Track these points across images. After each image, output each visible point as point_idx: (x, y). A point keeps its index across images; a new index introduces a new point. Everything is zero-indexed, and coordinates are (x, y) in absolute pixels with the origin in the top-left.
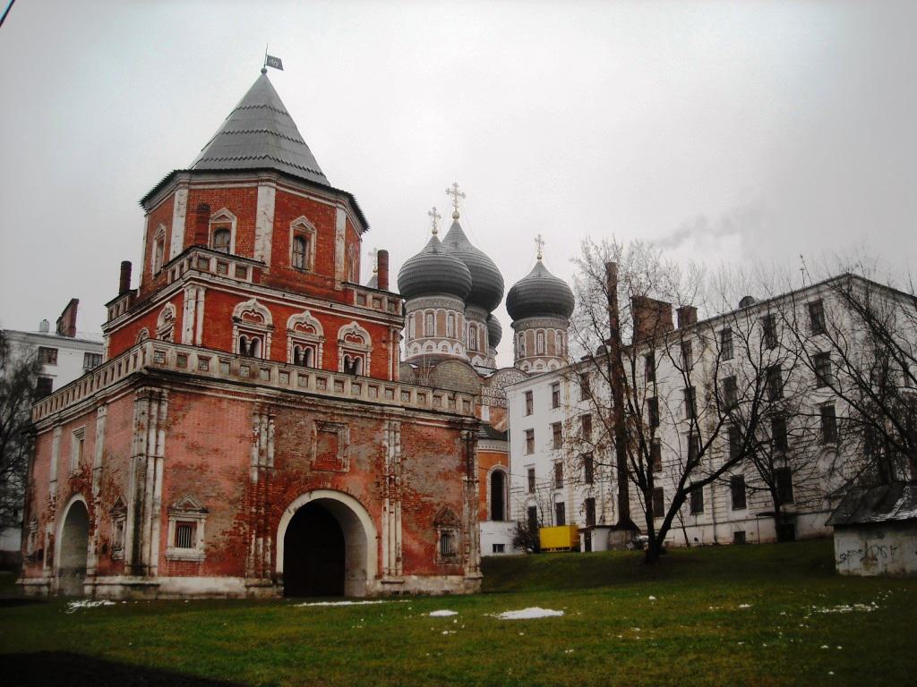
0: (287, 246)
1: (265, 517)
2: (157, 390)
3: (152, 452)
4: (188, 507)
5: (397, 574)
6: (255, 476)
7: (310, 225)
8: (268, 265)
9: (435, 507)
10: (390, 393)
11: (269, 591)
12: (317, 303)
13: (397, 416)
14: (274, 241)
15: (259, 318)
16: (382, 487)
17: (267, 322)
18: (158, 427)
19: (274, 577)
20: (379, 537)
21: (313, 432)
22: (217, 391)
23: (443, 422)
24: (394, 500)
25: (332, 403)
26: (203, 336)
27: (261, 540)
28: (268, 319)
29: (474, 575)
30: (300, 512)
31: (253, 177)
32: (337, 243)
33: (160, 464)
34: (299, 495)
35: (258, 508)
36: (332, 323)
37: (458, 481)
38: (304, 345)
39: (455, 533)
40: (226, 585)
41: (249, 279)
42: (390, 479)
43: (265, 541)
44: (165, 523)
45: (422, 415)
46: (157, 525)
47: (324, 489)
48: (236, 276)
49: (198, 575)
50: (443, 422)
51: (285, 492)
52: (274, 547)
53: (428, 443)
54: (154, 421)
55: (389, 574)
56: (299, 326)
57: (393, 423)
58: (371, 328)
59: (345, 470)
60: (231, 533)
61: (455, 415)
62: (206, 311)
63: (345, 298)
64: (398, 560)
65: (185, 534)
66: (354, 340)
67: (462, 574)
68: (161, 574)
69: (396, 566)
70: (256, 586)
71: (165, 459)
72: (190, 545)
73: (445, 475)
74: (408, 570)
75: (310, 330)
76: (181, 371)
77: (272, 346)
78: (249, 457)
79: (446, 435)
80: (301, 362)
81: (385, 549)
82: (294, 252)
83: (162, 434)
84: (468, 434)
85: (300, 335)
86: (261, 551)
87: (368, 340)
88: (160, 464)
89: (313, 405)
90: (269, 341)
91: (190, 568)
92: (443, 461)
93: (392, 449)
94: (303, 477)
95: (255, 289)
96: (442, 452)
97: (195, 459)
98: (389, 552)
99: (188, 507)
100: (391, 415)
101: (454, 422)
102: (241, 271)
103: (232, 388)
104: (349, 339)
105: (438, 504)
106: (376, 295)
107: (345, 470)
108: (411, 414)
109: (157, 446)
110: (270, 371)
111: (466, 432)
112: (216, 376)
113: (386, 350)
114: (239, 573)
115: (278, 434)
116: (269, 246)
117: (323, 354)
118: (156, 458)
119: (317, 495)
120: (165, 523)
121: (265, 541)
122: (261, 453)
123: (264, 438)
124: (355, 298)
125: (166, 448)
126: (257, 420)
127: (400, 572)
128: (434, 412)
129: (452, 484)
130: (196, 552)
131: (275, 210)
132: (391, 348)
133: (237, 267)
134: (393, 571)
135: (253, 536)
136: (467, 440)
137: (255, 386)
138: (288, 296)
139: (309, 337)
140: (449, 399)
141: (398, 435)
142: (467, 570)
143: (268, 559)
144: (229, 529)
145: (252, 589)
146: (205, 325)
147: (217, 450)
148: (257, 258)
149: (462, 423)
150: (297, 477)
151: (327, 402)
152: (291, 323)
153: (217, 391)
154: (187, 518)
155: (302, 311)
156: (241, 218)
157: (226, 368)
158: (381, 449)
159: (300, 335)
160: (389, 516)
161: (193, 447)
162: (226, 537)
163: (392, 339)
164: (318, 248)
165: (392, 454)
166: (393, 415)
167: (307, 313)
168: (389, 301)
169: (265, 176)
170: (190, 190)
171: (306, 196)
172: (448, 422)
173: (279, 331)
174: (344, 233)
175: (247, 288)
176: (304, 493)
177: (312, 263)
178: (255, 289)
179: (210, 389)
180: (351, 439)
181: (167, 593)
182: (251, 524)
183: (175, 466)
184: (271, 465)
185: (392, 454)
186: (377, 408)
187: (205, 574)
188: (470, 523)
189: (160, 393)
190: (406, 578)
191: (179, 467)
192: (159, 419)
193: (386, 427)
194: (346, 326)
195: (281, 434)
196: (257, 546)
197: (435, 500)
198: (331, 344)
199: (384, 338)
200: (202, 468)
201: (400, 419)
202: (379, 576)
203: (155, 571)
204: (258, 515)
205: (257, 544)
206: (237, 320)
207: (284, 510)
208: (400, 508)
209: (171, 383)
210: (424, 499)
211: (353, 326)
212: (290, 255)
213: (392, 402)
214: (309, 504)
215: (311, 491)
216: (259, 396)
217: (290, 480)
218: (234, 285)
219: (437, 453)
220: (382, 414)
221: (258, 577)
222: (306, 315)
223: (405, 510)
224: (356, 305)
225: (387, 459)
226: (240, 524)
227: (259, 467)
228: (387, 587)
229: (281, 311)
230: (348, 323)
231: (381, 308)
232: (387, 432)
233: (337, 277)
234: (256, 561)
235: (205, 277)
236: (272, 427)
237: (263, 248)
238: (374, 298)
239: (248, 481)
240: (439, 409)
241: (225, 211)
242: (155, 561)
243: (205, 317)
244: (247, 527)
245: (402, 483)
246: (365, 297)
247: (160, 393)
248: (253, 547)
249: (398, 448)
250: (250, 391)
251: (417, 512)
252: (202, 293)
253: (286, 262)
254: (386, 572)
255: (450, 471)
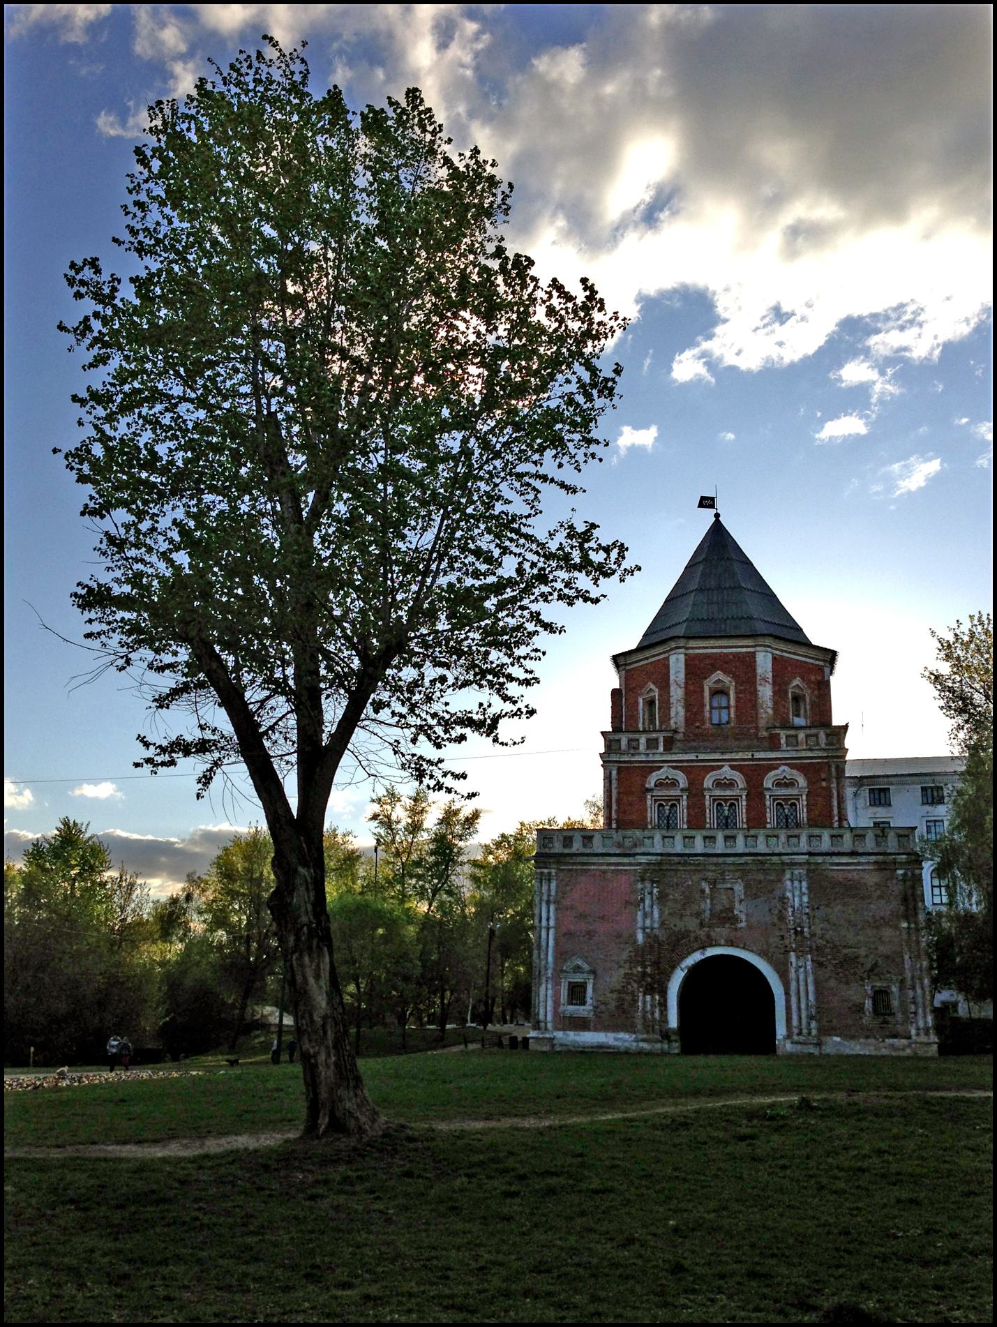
0: (703, 705)
1: (650, 976)
2: (546, 871)
3: (544, 923)
4: (577, 969)
5: (809, 1034)
6: (640, 937)
7: (727, 679)
8: (682, 730)
9: (861, 960)
10: (794, 840)
11: (658, 1046)
12: (734, 756)
13: (800, 864)
14: (688, 706)
15: (674, 783)
16: (787, 942)
17: (682, 786)
18: (548, 902)
19: (666, 1036)
20: (787, 994)
21: (703, 891)
22: (602, 864)
23: (868, 863)
24: (801, 954)
25: (721, 860)
26: (617, 812)
27: (648, 998)
28: (682, 780)
29: (923, 1039)
30: (694, 971)
31: (659, 650)
32: (759, 688)
33: (552, 932)
34: (689, 954)
35: (644, 967)
36: (754, 774)
37: (897, 927)
38: (726, 801)
39: (894, 989)
40: (616, 1039)
41: (661, 749)
42: (796, 932)
43: (653, 998)
44: (557, 984)
45: (836, 860)
46: (550, 986)
47: (720, 945)
48: (648, 748)
49: (589, 1030)
50: (868, 863)
51: (673, 951)
52: (663, 1005)
53: (851, 889)
54: (545, 898)
55: (800, 1034)
56: (719, 784)
57: (796, 872)
58: (802, 768)
59: (740, 925)
60: (619, 992)
61: (885, 854)
62: (618, 787)
63: (774, 744)
64: (811, 1018)
65: (577, 992)
66: (786, 785)
67: (909, 1038)
68: (556, 1029)
69: (809, 1024)
70: (644, 1040)
71: (557, 928)
72: (584, 1003)
73: (878, 924)
74: (825, 1031)
75: (731, 784)
76: (566, 851)
77: (688, 807)
78: (635, 920)
79: (872, 879)
80: (726, 823)
81: (794, 1007)
82: (711, 708)
83: (552, 908)
84: (905, 874)
85: (718, 792)
86: (649, 1007)
87: (802, 781)
88: (552, 932)
89: (699, 865)
90: (685, 803)
91: (581, 1024)
92: (872, 906)
93: (797, 899)
94: (693, 935)
95: (664, 758)
96: (870, 897)
97: (583, 926)
98: (799, 1009)
99: (577, 969)
100: (793, 864)
101: (885, 863)
102: (652, 744)
103: (614, 860)
104: (779, 785)
105: (867, 956)
106: (808, 732)
107: (740, 925)
108: (820, 859)
109: (548, 919)
110: (652, 838)
111: (900, 872)
112: (600, 851)
113: (829, 789)
114: (630, 1028)
115: (662, 898)
116: (682, 711)
117: (747, 805)
118: (548, 929)
119: (711, 952)
120: (557, 984)
121: (653, 998)
122: (645, 916)
123: (647, 902)
124: (783, 741)
125: (557, 919)
126: (640, 886)
127: (814, 1032)
128: (853, 854)
129: (887, 933)
130: (584, 1011)
131: (686, 674)
132: (834, 785)
133: (648, 740)
134: (805, 1031)
135: (641, 994)
136: (904, 881)
137: (635, 855)
138: (701, 757)
139: (728, 793)
140: (877, 836)
141: (804, 884)
142: (913, 1032)
143: (657, 1015)
144: (618, 987)
145: (641, 1044)
146: (618, 801)
147: (603, 918)
148: (673, 726)
149: (895, 862)
150: (685, 934)
151: (714, 860)
152: (708, 782)
153: (602, 864)
154: (578, 978)
155: (720, 767)
156: (660, 689)
157: (608, 842)
158: (783, 899)
159: (718, 792)
160: (797, 971)
161: (582, 916)
162: (615, 996)
163: (834, 773)
164: (738, 700)
165: (797, 905)
166: (795, 864)
167: (726, 769)
168: (827, 735)
169: (673, 644)
170: (627, 671)
171: (718, 651)
172: (876, 863)
173: (695, 792)
174: (770, 675)
175: (658, 758)
176: (694, 951)
177: (732, 715)
178: (669, 758)
179: (594, 864)
180: (745, 893)
181: (561, 1045)
182: (639, 983)
183: (565, 935)
184: (656, 925)
185: (797, 905)
186: (775, 859)
187: (596, 1030)
188: (913, 978)
189: (549, 874)
190: (823, 1039)
191: (569, 934)
192: (549, 896)
193: (788, 876)
194: (773, 773)
195: (667, 895)
196: (644, 1002)
197: (863, 952)
198: (755, 793)
199: (823, 776)
200: (590, 934)
201: (806, 867)
202: (789, 1036)
203: (550, 1026)
204: (644, 974)
205: (645, 1001)
206: (651, 790)
207: (673, 967)
208: (809, 963)
209: (558, 862)
210: (845, 951)
211: (784, 771)
212: (707, 714)
213: (795, 850)
214: (702, 961)
215: (703, 948)
216: (640, 864)
217: (679, 940)
218: (643, 758)
219: (863, 898)
220: (783, 863)
221: (648, 1032)
222: (727, 772)
223: (819, 964)
224: (784, 747)
225: (790, 910)
226: (629, 983)
227: (644, 929)
228: (799, 1047)
229: (695, 773)
230: (776, 768)
231: (818, 744)
232: (789, 883)
233: (762, 723)
234: (644, 1017)
235: (614, 758)
236: (655, 891)
237: (678, 713)
238: (807, 736)
239: (635, 942)
240: (861, 851)
241: (652, 687)
242: (549, 1018)
243: (619, 793)
244: (635, 985)
245: (813, 935)
246: (796, 736)
247: (549, 874)
248: (640, 1004)
249: (805, 899)
250: (631, 860)
251: (835, 966)
252: (614, 773)
253: (703, 723)
254: (796, 1031)
255: (882, 918)
